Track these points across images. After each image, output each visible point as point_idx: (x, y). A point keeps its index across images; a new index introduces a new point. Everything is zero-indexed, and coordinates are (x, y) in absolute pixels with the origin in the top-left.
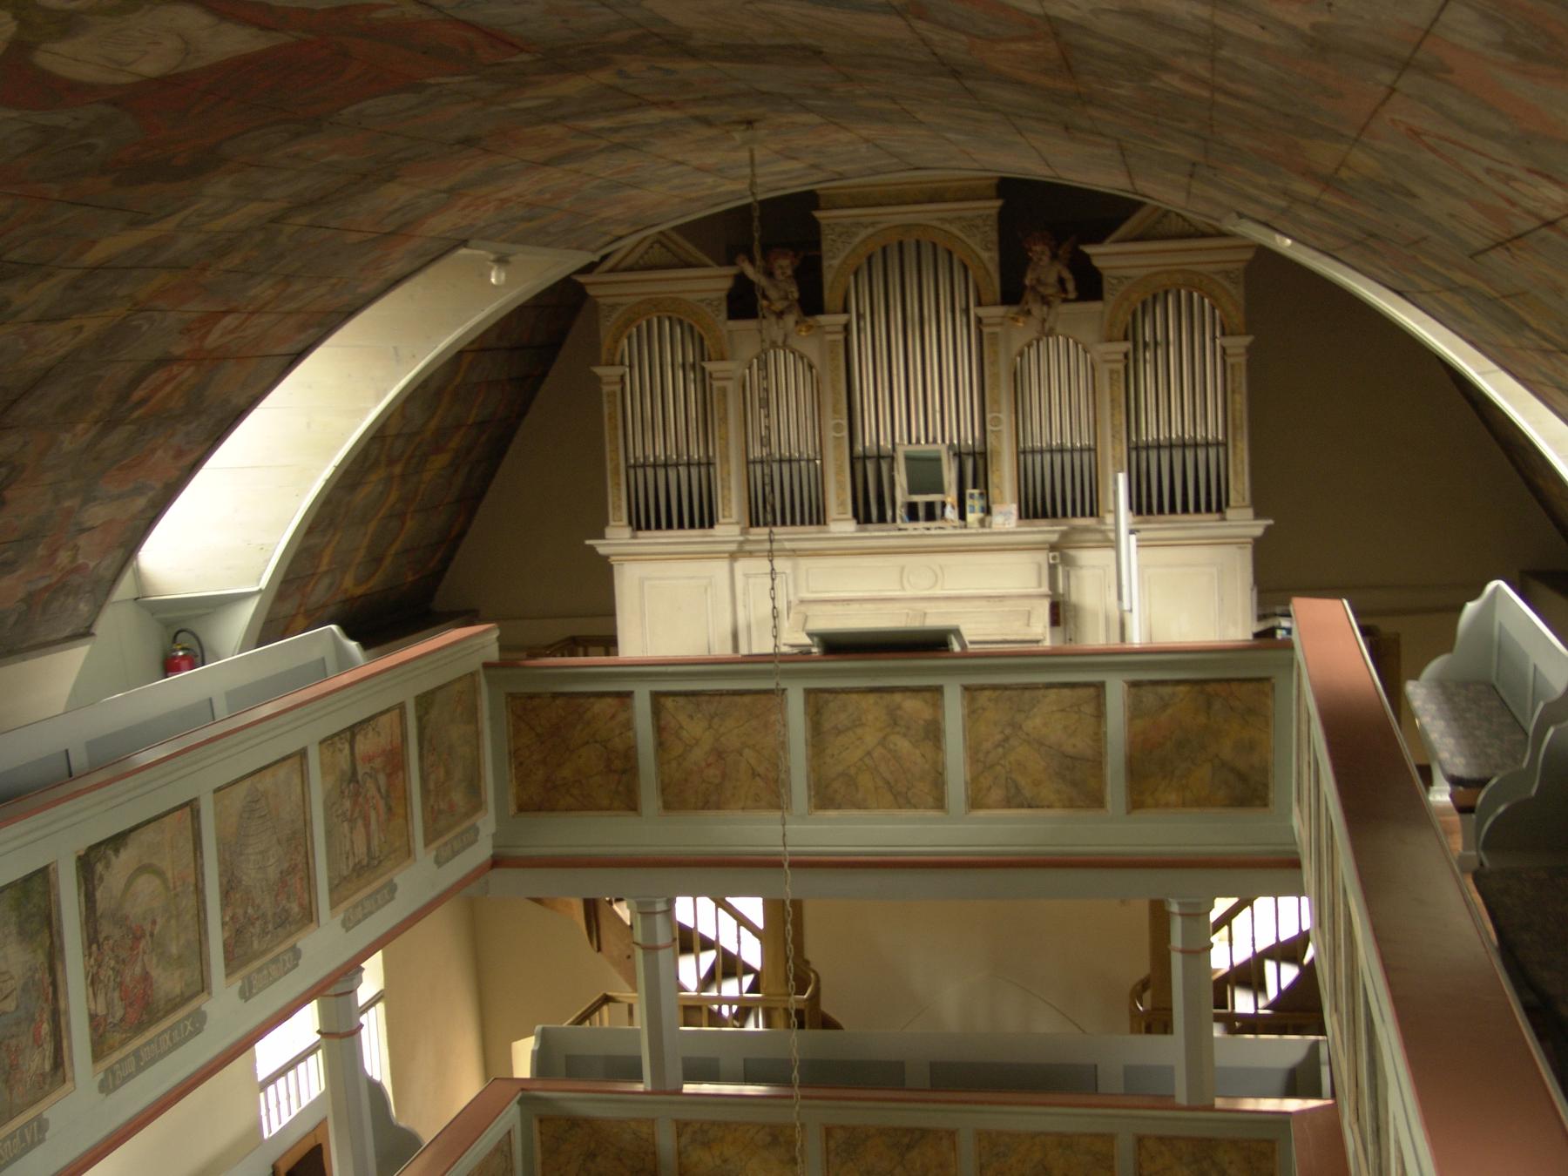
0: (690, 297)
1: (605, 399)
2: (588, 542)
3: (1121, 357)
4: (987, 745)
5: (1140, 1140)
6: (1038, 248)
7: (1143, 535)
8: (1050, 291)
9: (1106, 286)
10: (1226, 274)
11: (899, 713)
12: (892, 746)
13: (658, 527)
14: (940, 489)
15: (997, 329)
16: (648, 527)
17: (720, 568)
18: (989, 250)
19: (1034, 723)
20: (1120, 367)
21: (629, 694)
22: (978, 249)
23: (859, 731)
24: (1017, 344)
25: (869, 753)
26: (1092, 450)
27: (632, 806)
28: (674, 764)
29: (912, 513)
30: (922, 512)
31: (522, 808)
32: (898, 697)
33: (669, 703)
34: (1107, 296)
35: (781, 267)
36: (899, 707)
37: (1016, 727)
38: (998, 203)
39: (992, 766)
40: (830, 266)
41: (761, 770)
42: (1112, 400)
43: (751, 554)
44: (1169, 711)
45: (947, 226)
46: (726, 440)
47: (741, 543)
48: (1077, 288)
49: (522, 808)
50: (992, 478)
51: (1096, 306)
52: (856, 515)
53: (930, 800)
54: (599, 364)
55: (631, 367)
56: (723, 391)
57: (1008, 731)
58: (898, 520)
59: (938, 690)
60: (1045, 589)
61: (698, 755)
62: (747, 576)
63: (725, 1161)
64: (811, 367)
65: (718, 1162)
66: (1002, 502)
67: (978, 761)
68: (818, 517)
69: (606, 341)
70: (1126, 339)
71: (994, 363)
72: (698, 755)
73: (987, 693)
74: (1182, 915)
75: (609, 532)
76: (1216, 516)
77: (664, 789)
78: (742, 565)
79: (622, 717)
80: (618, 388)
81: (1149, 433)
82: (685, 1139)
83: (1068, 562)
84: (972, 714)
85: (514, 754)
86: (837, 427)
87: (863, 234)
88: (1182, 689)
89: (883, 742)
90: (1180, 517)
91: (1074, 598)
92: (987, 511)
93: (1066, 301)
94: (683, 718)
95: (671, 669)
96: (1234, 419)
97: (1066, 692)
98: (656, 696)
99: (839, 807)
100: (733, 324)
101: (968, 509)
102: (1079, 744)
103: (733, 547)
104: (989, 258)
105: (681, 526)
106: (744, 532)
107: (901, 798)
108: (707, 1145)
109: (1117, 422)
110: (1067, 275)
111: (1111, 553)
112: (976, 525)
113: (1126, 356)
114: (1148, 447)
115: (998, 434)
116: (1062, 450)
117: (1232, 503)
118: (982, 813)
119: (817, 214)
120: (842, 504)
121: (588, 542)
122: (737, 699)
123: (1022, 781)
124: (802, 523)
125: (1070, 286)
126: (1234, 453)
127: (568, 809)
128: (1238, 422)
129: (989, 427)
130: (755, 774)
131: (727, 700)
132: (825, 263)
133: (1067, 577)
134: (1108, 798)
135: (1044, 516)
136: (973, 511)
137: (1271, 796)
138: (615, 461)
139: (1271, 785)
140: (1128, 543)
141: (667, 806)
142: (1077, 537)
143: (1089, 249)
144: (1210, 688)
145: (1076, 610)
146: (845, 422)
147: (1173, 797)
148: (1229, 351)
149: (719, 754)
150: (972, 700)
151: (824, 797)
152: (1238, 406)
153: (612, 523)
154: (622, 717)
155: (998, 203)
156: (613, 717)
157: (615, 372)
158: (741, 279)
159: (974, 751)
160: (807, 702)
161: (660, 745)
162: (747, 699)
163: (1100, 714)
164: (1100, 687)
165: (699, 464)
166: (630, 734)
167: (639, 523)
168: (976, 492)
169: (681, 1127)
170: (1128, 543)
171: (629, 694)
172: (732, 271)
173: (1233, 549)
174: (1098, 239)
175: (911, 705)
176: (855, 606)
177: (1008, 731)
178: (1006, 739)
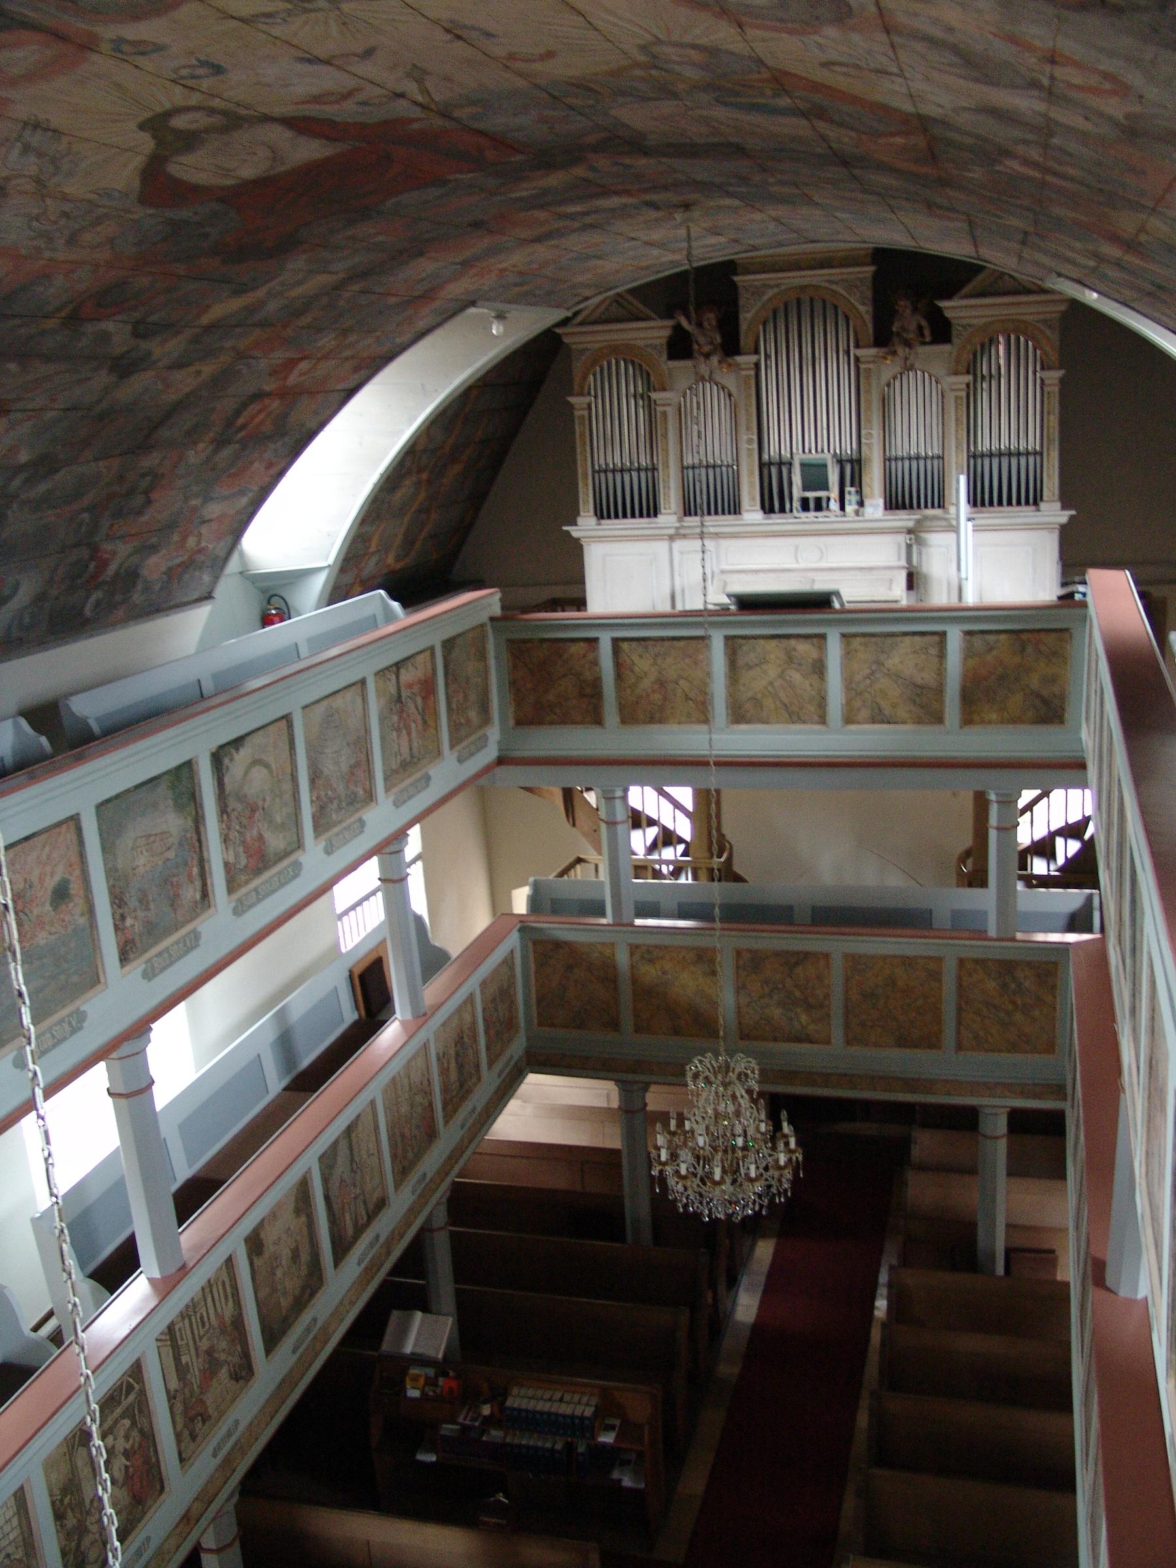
0: (641, 343)
1: (577, 421)
2: (565, 528)
3: (964, 386)
4: (858, 678)
5: (961, 962)
6: (902, 303)
7: (978, 522)
8: (911, 336)
9: (954, 332)
10: (1045, 322)
11: (794, 653)
12: (788, 678)
13: (617, 517)
14: (826, 487)
15: (871, 366)
16: (609, 517)
17: (662, 547)
18: (864, 304)
19: (894, 661)
20: (964, 394)
21: (596, 640)
22: (856, 304)
23: (764, 667)
24: (886, 375)
25: (771, 683)
26: (941, 458)
27: (598, 721)
28: (628, 691)
29: (805, 505)
30: (812, 505)
31: (519, 723)
32: (793, 642)
33: (625, 646)
34: (955, 340)
35: (708, 319)
36: (794, 649)
37: (879, 663)
38: (872, 268)
39: (861, 693)
40: (745, 319)
41: (692, 695)
42: (957, 420)
43: (684, 536)
44: (994, 653)
45: (834, 287)
46: (666, 451)
47: (677, 528)
48: (932, 334)
49: (519, 723)
50: (865, 479)
51: (946, 348)
52: (763, 507)
53: (816, 718)
54: (572, 395)
55: (596, 397)
56: (664, 414)
57: (874, 667)
58: (794, 511)
59: (823, 637)
60: (903, 563)
61: (646, 684)
62: (682, 553)
63: (665, 973)
64: (730, 395)
65: (660, 973)
66: (872, 497)
67: (853, 689)
68: (735, 509)
69: (577, 380)
70: (968, 372)
71: (868, 391)
72: (646, 684)
73: (859, 639)
74: (997, 802)
75: (580, 520)
76: (1033, 508)
77: (621, 707)
78: (678, 545)
79: (591, 656)
80: (586, 413)
81: (984, 445)
82: (637, 957)
83: (920, 542)
84: (848, 654)
85: (513, 683)
86: (750, 441)
87: (770, 293)
88: (1003, 637)
89: (781, 676)
90: (1006, 509)
91: (924, 569)
92: (861, 504)
93: (924, 343)
94: (635, 658)
95: (626, 621)
96: (1048, 434)
97: (917, 639)
98: (616, 641)
99: (749, 722)
100: (672, 364)
101: (847, 502)
102: (927, 677)
103: (672, 531)
104: (865, 310)
105: (633, 516)
106: (680, 520)
107: (794, 716)
108: (651, 961)
109: (960, 437)
110: (924, 323)
111: (953, 536)
112: (853, 514)
113: (968, 385)
114: (982, 456)
115: (870, 446)
116: (918, 458)
117: (1045, 498)
118: (853, 727)
119: (736, 279)
120: (753, 499)
121: (565, 528)
122: (675, 643)
123: (883, 704)
124: (723, 513)
125: (927, 332)
126: (1048, 459)
127: (552, 723)
128: (1051, 437)
129: (863, 440)
130: (687, 698)
131: (667, 643)
132: (741, 317)
133: (920, 553)
134: (947, 716)
135: (904, 507)
136: (850, 504)
137: (1066, 715)
138: (584, 468)
139: (1067, 707)
140: (966, 527)
141: (624, 721)
142: (928, 523)
143: (943, 304)
144: (1024, 637)
145: (926, 578)
146: (755, 437)
147: (994, 716)
148: (1047, 382)
149: (661, 683)
150: (848, 644)
151: (738, 715)
152: (1051, 424)
153: (582, 514)
154: (591, 656)
155: (872, 268)
156: (584, 656)
157: (584, 400)
158: (678, 328)
159: (849, 684)
160: (726, 645)
161: (619, 677)
162: (682, 643)
163: (942, 655)
164: (943, 635)
165: (646, 470)
166: (597, 668)
167: (602, 513)
168: (853, 490)
169: (633, 948)
170: (966, 527)
171: (596, 640)
172: (669, 323)
173: (1044, 533)
174: (949, 297)
175: (803, 647)
176: (762, 575)
177: (874, 667)
178: (873, 673)
